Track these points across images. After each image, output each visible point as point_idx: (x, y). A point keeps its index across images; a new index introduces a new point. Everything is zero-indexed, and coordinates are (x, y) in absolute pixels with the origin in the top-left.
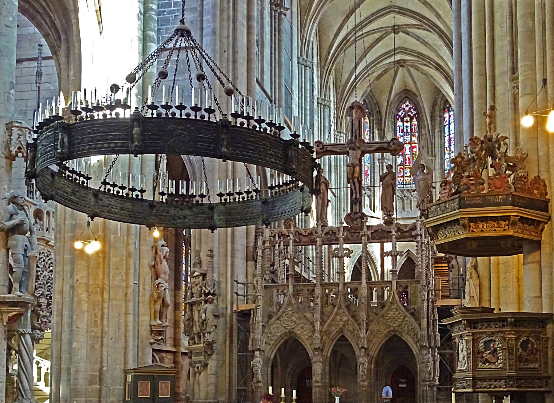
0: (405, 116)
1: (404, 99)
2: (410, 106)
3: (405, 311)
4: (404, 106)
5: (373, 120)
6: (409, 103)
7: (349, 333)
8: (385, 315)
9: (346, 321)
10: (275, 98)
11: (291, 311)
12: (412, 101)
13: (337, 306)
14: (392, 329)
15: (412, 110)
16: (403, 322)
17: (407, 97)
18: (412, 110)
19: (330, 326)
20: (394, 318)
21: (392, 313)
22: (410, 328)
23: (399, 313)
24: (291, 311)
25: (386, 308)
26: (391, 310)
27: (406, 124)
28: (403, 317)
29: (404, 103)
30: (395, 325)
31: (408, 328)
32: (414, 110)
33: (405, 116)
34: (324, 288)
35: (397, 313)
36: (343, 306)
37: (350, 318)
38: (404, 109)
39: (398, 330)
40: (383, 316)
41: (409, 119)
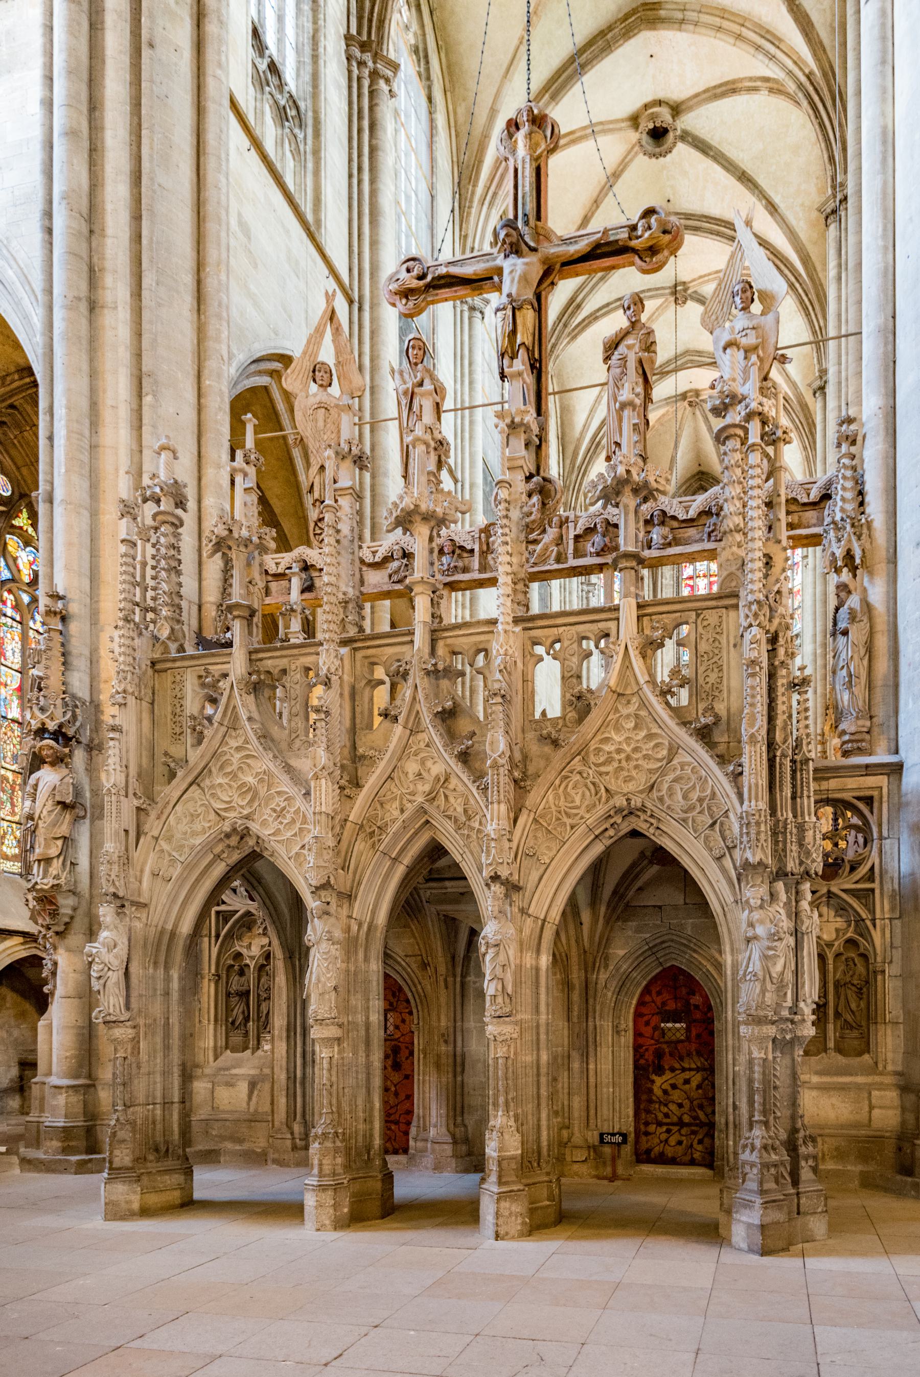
3: (672, 723)
7: (449, 826)
8: (593, 746)
9: (437, 779)
11: (238, 749)
13: (401, 719)
14: (620, 801)
16: (663, 772)
19: (378, 800)
20: (628, 758)
21: (617, 738)
22: (695, 796)
23: (650, 736)
24: (238, 749)
25: (594, 719)
26: (618, 728)
28: (665, 752)
30: (631, 787)
31: (685, 797)
34: (360, 654)
35: (643, 734)
36: (426, 718)
37: (452, 762)
39: (643, 809)
40: (582, 752)
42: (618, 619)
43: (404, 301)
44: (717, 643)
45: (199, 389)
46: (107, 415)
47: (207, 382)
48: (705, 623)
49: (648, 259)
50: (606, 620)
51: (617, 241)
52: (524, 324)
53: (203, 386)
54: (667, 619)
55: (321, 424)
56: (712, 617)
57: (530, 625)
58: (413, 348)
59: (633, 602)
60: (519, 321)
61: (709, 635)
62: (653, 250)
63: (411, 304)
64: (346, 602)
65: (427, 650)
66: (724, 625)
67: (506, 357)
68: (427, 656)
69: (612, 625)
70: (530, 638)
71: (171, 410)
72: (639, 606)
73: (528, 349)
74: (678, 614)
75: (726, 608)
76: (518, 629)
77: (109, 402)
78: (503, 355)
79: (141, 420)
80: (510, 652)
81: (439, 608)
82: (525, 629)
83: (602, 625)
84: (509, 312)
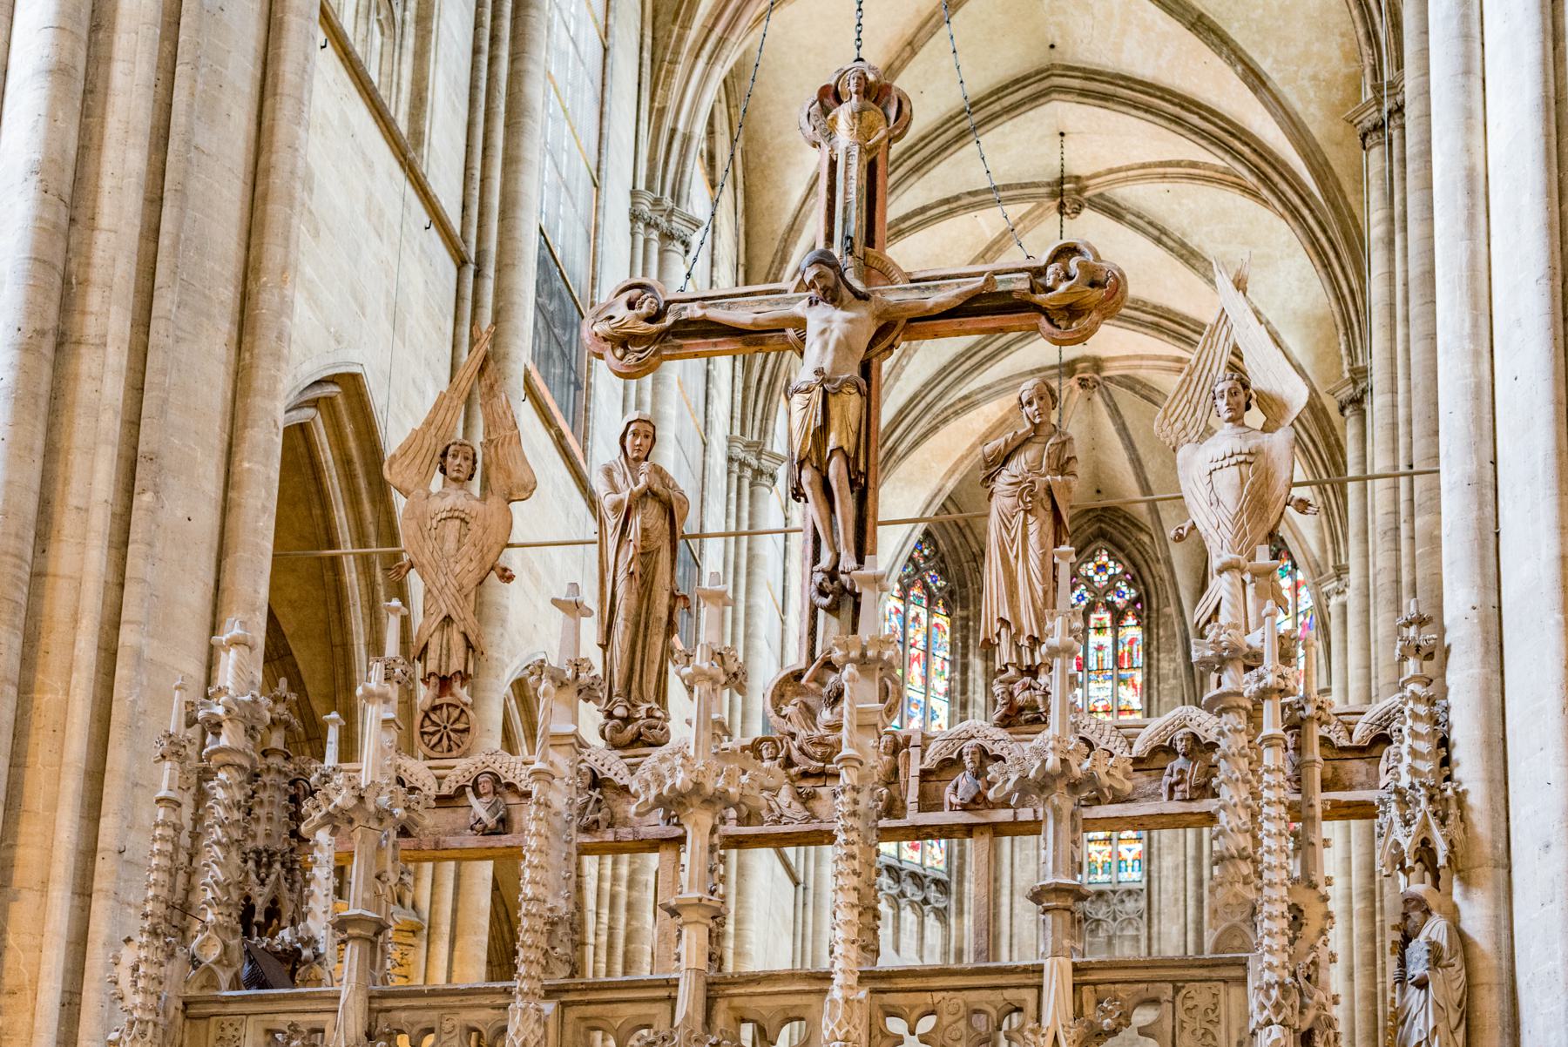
0: (1091, 608)
1: (1089, 542)
2: (1114, 568)
4: (1089, 569)
5: (967, 619)
6: (1111, 555)
10: (480, 254)
12: (1121, 548)
15: (1122, 586)
17: (1102, 535)
18: (1122, 586)
27: (1094, 639)
29: (1092, 557)
32: (1129, 585)
33: (1091, 608)
38: (1089, 579)
41: (1107, 617)
42: (1040, 987)
43: (619, 352)
44: (1209, 1038)
45: (228, 472)
46: (67, 523)
47: (246, 465)
48: (1189, 1004)
49: (1063, 324)
50: (1018, 987)
51: (1010, 292)
52: (843, 417)
53: (235, 469)
54: (1122, 991)
55: (451, 545)
56: (1200, 996)
57: (884, 986)
58: (635, 434)
59: (1067, 964)
60: (835, 412)
61: (1198, 1024)
62: (1073, 311)
63: (631, 359)
64: (553, 924)
65: (699, 1018)
66: (1222, 1009)
67: (807, 465)
68: (699, 1031)
69: (1029, 996)
70: (881, 1007)
71: (180, 513)
72: (1077, 969)
73: (847, 458)
74: (1144, 986)
75: (1225, 982)
76: (863, 993)
77: (73, 501)
78: (801, 464)
79: (127, 532)
80: (854, 1036)
81: (718, 944)
82: (873, 991)
83: (1008, 994)
84: (817, 397)
